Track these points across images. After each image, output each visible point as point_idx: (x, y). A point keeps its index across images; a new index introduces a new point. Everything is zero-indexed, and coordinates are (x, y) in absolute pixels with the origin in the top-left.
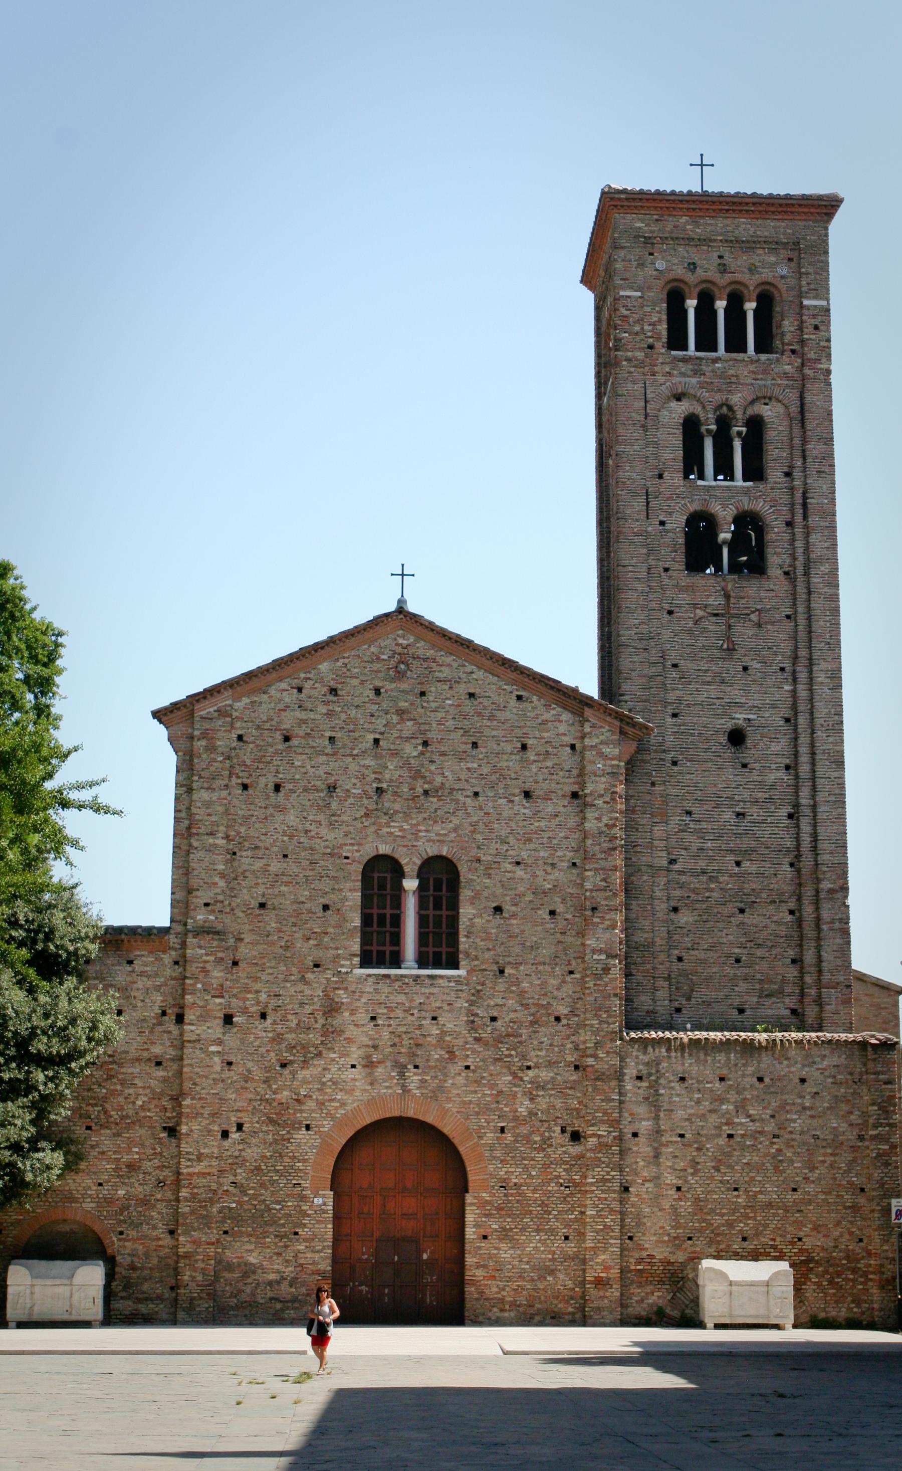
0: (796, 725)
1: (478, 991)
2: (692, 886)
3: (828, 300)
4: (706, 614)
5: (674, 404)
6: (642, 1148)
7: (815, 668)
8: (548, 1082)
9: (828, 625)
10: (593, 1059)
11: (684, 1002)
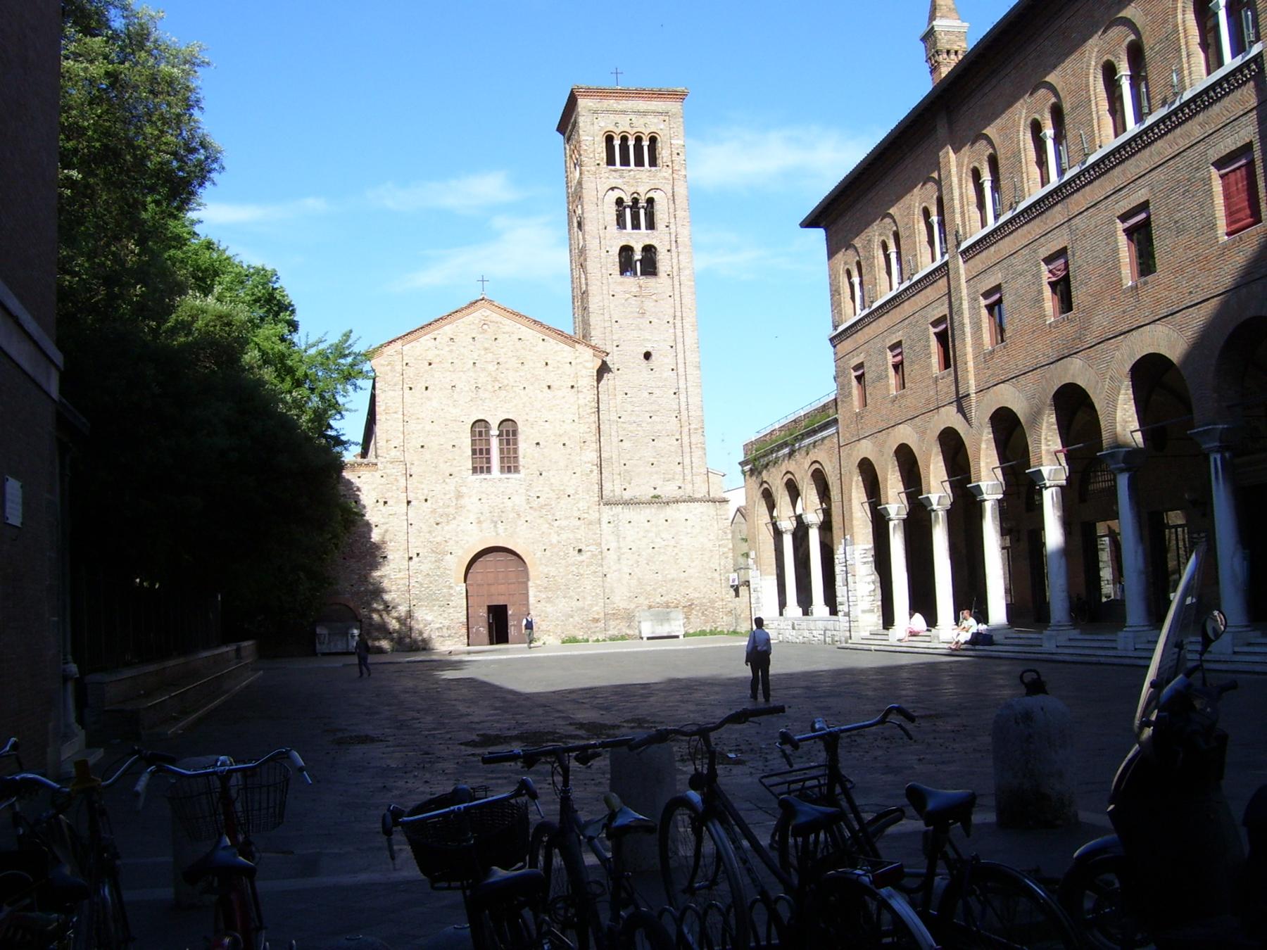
6: (612, 556)
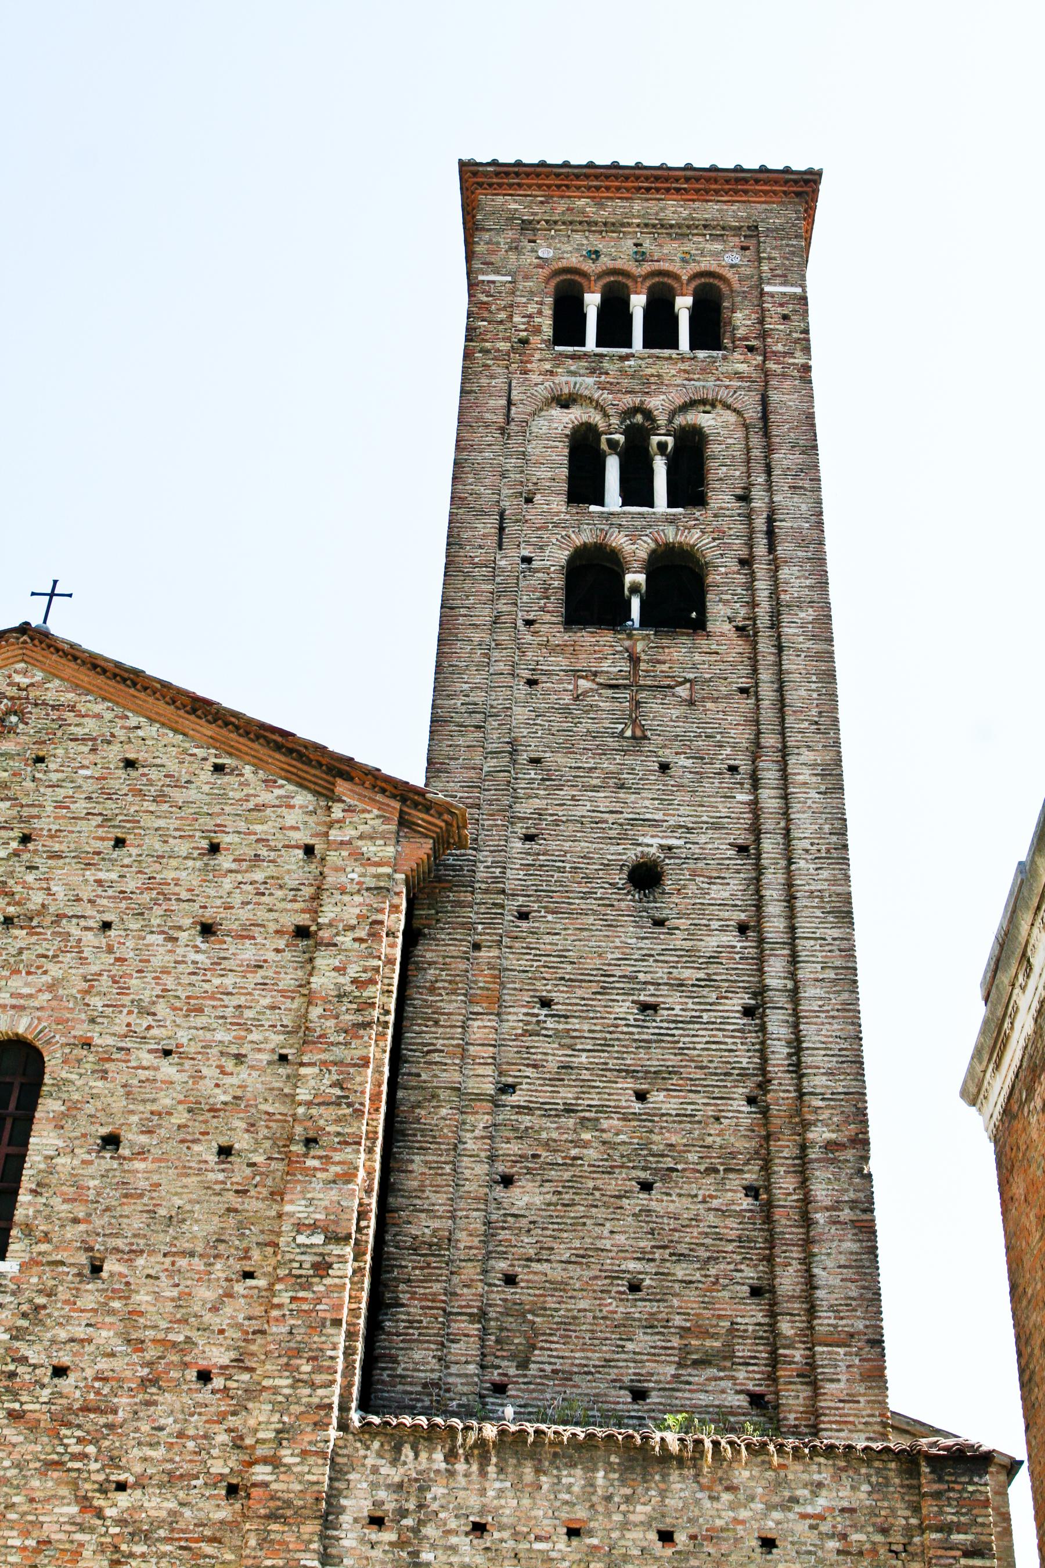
0: (758, 857)
1: (38, 1308)
2: (544, 1135)
3: (804, 287)
4: (595, 687)
5: (556, 412)
7: (792, 760)
8: (161, 1523)
9: (815, 695)
10: (269, 1469)
11: (512, 1371)
